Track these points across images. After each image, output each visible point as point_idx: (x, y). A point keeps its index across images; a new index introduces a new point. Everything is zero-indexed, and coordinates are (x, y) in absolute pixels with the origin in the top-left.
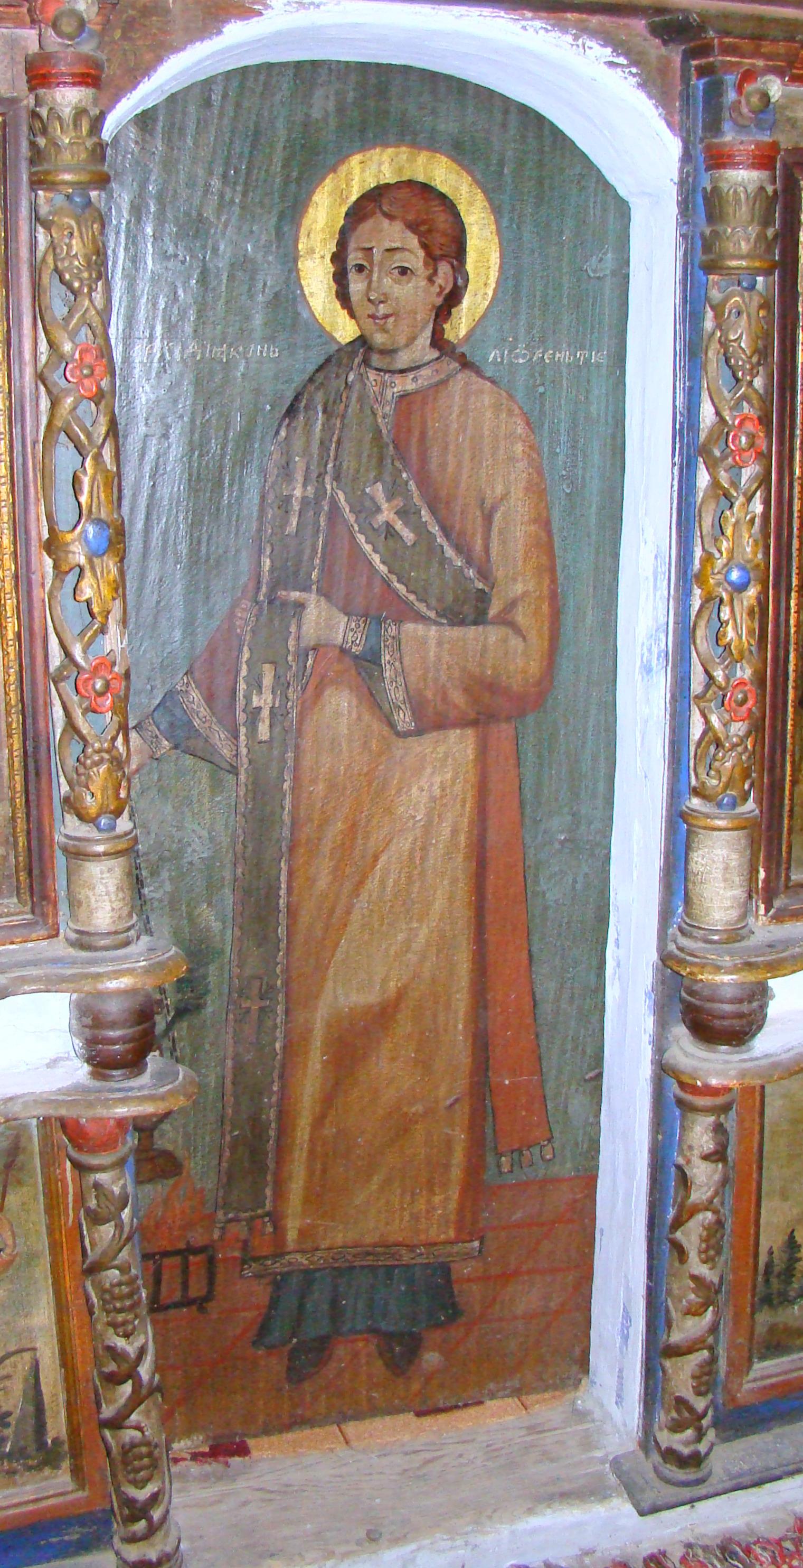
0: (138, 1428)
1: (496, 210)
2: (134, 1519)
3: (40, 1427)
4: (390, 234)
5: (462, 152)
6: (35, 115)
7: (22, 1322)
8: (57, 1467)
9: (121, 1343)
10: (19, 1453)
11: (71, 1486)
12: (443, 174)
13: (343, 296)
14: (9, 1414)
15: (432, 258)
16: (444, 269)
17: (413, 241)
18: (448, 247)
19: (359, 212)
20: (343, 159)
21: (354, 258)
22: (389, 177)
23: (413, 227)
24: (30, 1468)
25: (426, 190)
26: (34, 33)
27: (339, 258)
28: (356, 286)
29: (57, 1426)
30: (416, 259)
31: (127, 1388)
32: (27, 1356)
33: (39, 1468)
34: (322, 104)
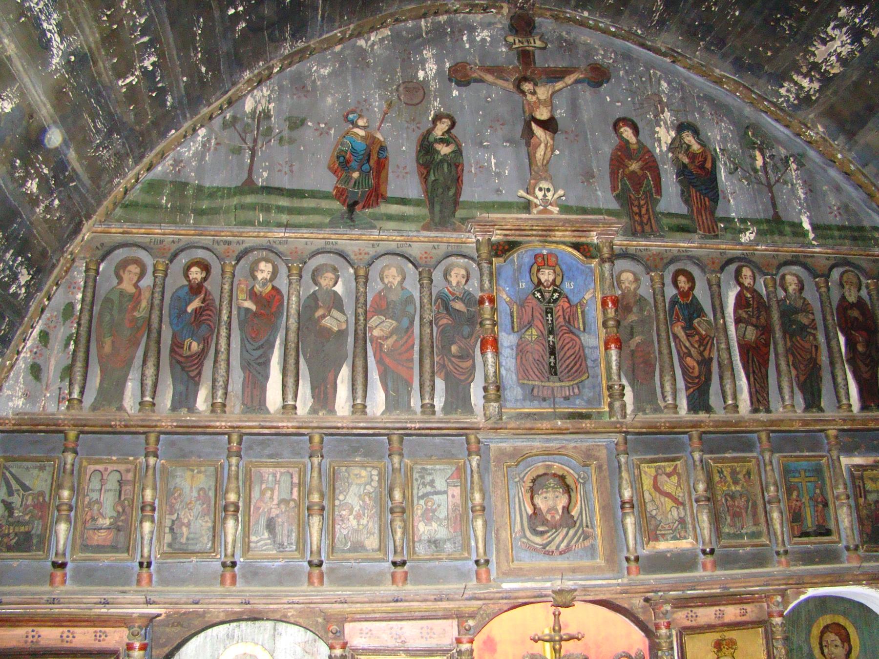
1: (856, 628)
4: (831, 637)
5: (845, 614)
6: (771, 624)
12: (841, 620)
13: (823, 653)
15: (843, 641)
16: (846, 645)
17: (837, 638)
18: (846, 638)
19: (823, 633)
20: (818, 618)
21: (824, 643)
22: (829, 622)
23: (836, 634)
25: (838, 625)
26: (765, 605)
27: (821, 644)
28: (826, 650)
30: (839, 642)
34: (811, 606)
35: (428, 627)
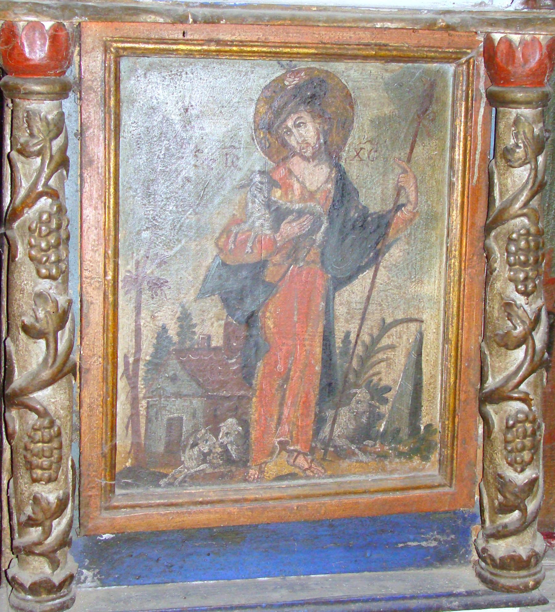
0: (525, 400)
2: (506, 509)
3: (415, 411)
7: (413, 289)
8: (425, 458)
9: (521, 300)
10: (392, 435)
11: (439, 479)
14: (388, 389)
24: (400, 454)
29: (432, 413)
31: (520, 354)
32: (413, 326)
33: (408, 455)
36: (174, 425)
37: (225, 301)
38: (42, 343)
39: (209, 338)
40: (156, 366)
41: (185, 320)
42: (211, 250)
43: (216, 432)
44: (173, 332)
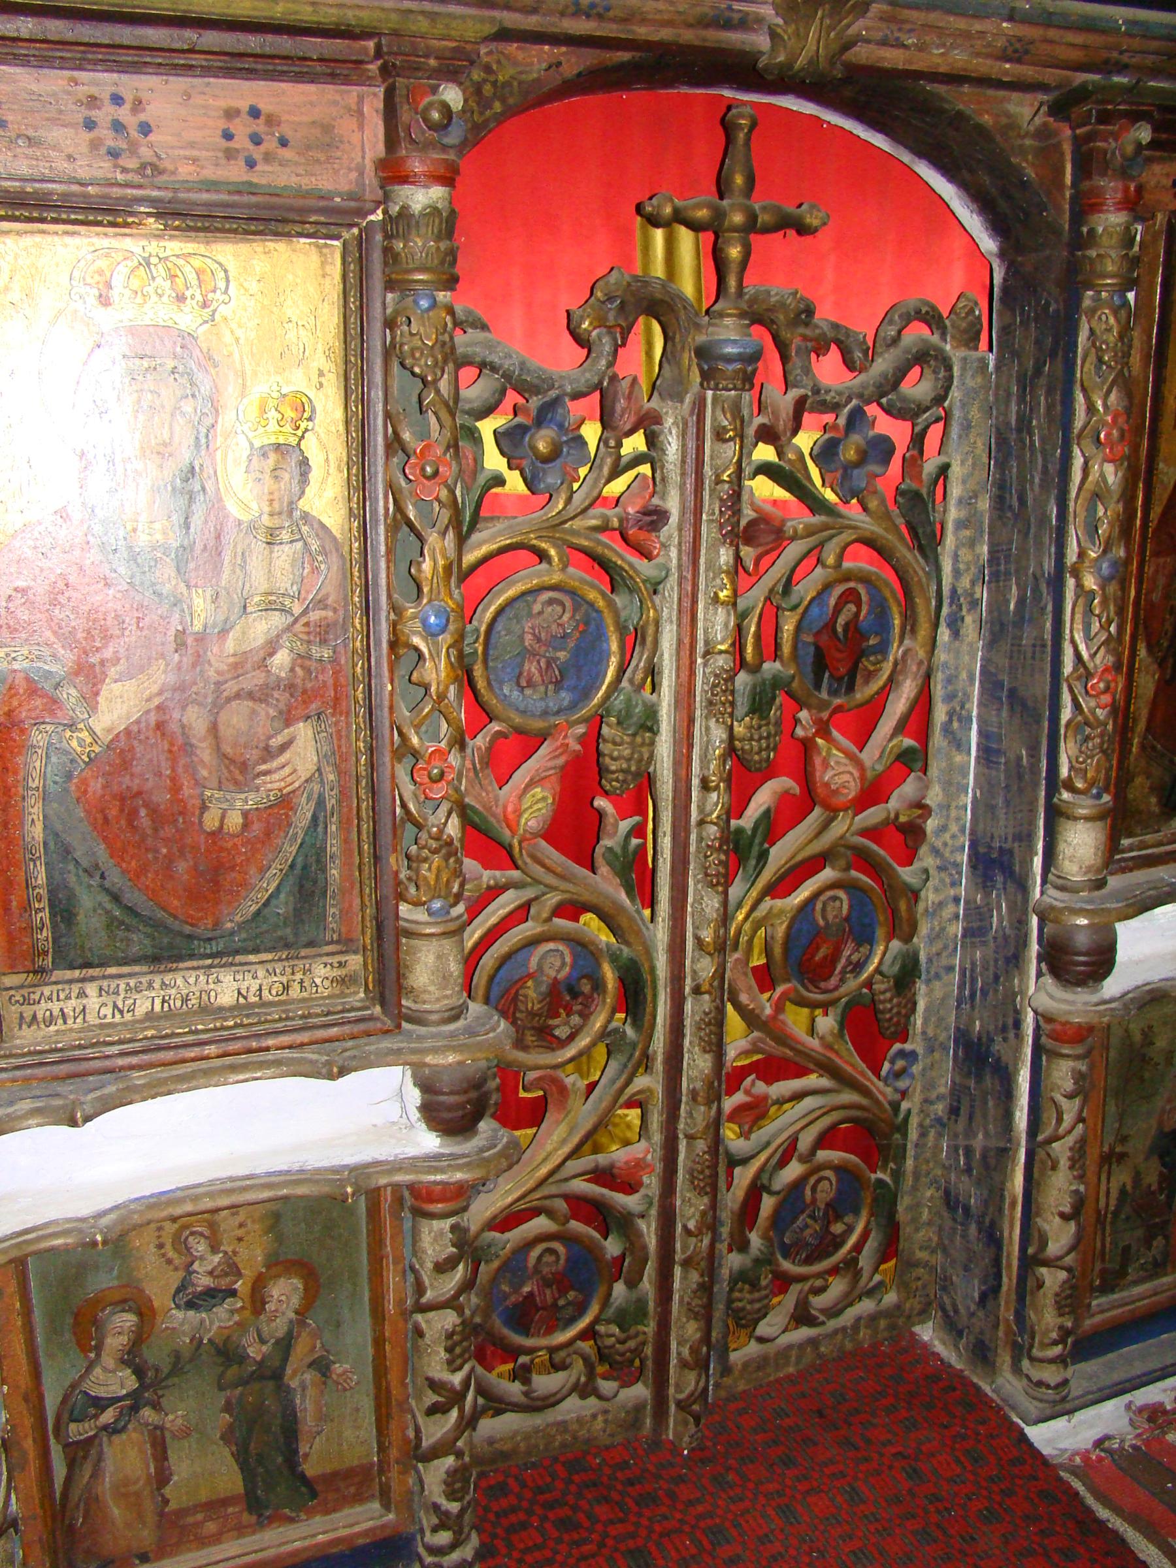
35: (255, 113)
36: (1126, 1250)
37: (1161, 1157)
38: (1073, 1224)
39: (1150, 1186)
40: (1116, 1214)
41: (1137, 1178)
42: (1154, 1123)
43: (1149, 1249)
44: (1129, 1188)
